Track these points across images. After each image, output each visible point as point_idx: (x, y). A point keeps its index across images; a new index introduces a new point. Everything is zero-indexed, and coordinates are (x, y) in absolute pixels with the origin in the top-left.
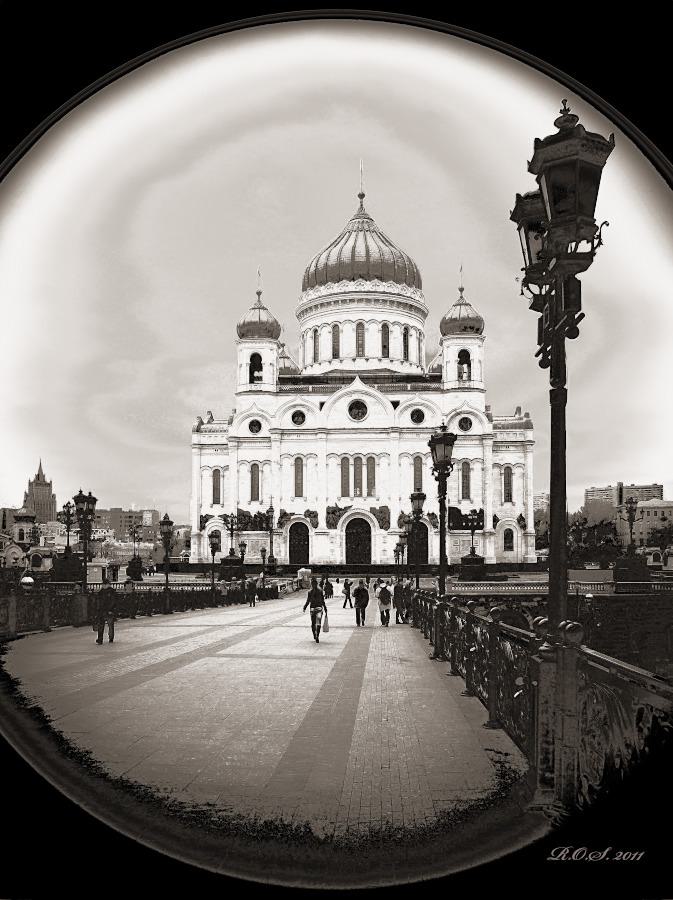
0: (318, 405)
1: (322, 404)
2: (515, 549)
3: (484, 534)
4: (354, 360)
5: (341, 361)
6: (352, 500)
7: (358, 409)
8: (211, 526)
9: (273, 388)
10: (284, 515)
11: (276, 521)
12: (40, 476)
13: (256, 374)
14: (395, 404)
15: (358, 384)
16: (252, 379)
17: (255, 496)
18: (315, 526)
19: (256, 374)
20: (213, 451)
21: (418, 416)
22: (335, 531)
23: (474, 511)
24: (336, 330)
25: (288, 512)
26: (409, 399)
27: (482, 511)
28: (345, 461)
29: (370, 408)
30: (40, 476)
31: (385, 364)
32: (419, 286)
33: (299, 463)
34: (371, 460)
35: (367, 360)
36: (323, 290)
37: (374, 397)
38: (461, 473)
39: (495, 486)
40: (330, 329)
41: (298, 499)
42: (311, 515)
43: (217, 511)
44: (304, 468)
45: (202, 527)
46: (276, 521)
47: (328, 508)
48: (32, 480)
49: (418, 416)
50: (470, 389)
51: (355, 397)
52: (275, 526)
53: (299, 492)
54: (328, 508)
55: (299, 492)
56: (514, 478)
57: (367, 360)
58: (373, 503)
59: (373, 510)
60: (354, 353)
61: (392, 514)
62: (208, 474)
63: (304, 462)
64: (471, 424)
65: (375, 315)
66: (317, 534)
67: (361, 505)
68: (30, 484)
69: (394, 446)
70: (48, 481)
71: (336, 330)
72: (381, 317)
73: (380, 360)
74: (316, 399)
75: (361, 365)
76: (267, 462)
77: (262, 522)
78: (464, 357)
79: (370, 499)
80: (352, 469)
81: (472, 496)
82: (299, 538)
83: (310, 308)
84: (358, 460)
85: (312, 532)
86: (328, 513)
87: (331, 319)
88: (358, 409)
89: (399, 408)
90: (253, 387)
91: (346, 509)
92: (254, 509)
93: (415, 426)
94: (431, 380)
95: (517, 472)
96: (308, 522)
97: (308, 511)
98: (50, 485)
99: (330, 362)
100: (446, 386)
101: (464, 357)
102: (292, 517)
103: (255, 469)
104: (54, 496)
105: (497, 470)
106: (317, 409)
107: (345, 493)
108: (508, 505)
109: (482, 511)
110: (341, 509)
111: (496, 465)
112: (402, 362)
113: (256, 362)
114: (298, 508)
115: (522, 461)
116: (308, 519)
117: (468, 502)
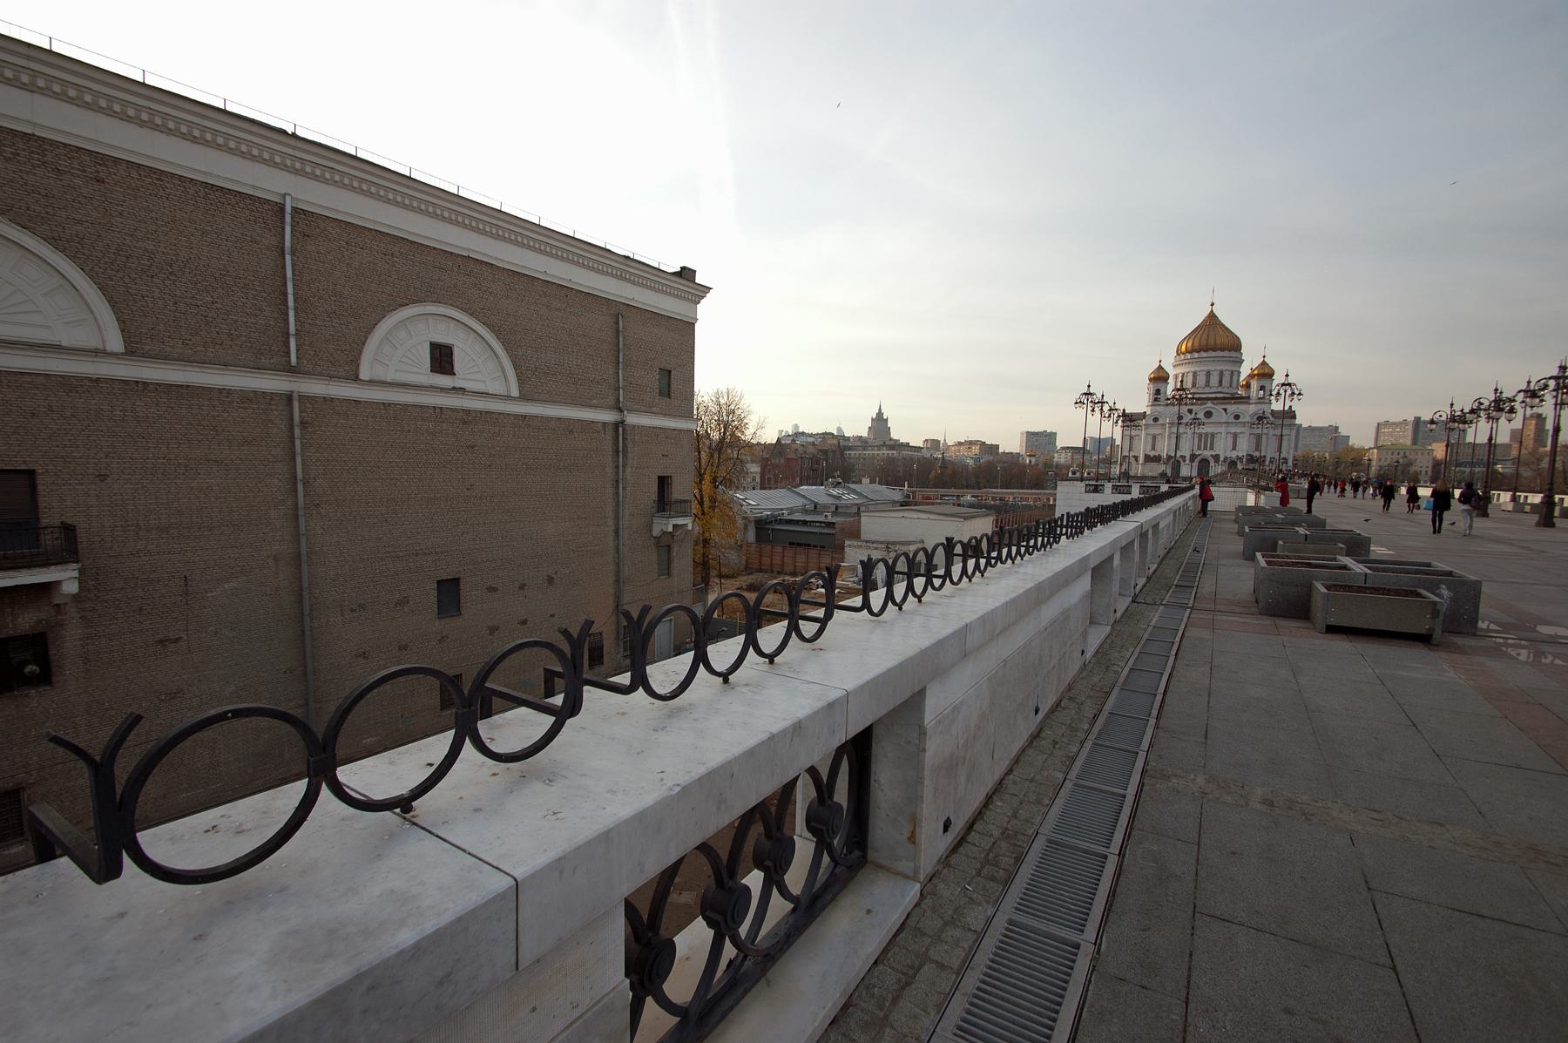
7: (1208, 414)
12: (880, 414)
14: (1225, 410)
15: (1209, 404)
17: (1153, 449)
21: (1237, 417)
26: (1232, 408)
29: (1214, 414)
30: (880, 414)
31: (1220, 389)
34: (1213, 435)
39: (1274, 443)
40: (1191, 374)
42: (1183, 457)
48: (874, 417)
49: (1237, 417)
51: (1207, 410)
59: (1212, 456)
65: (1215, 368)
67: (1207, 453)
68: (873, 419)
69: (1223, 429)
70: (885, 417)
72: (1219, 368)
75: (1207, 390)
76: (1158, 435)
77: (1157, 459)
82: (1176, 466)
85: (1182, 463)
88: (1208, 414)
90: (1156, 403)
91: (1199, 455)
92: (1152, 454)
94: (1245, 400)
103: (1154, 437)
105: (1274, 437)
106: (1188, 414)
107: (1199, 449)
111: (1274, 435)
113: (1158, 392)
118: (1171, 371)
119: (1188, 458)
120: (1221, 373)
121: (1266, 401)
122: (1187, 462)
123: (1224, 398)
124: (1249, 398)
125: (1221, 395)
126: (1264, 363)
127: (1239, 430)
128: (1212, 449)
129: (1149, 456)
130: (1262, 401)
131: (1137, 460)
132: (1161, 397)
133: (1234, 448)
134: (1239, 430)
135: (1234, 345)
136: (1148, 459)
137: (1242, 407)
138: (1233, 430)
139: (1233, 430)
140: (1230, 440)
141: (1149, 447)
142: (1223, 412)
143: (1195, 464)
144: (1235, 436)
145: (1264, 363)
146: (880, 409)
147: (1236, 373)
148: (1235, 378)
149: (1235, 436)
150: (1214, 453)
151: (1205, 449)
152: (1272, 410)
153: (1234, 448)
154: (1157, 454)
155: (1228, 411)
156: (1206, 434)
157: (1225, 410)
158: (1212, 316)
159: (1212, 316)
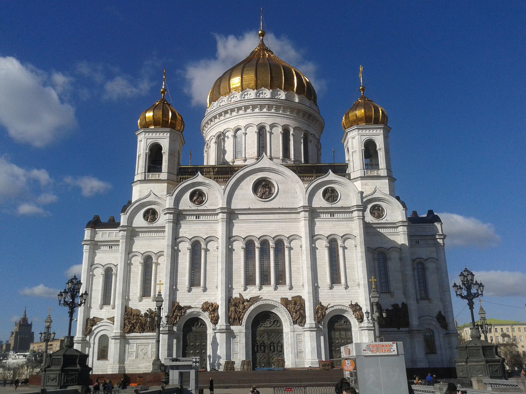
2: (439, 352)
3: (410, 332)
5: (245, 160)
6: (260, 288)
11: (164, 314)
12: (25, 320)
18: (215, 321)
20: (107, 248)
22: (239, 327)
23: (395, 306)
25: (182, 304)
27: (404, 305)
28: (249, 246)
30: (25, 320)
34: (279, 244)
38: (376, 263)
41: (194, 289)
46: (164, 314)
48: (18, 322)
50: (379, 177)
52: (164, 320)
56: (428, 273)
57: (271, 159)
58: (284, 292)
59: (285, 302)
60: (256, 155)
62: (99, 273)
64: (383, 210)
70: (30, 323)
79: (280, 288)
81: (392, 290)
84: (264, 243)
93: (329, 206)
95: (430, 265)
96: (205, 317)
97: (206, 303)
98: (30, 326)
102: (188, 311)
104: (33, 333)
107: (249, 281)
108: (425, 303)
109: (404, 305)
110: (244, 301)
115: (434, 255)
116: (206, 314)
117: (388, 295)
119: (221, 312)
122: (222, 322)
128: (280, 279)
129: (137, 314)
130: (375, 173)
143: (239, 330)
146: (25, 315)
147: (310, 138)
150: (289, 295)
151: (265, 280)
154: (153, 306)
156: (264, 243)
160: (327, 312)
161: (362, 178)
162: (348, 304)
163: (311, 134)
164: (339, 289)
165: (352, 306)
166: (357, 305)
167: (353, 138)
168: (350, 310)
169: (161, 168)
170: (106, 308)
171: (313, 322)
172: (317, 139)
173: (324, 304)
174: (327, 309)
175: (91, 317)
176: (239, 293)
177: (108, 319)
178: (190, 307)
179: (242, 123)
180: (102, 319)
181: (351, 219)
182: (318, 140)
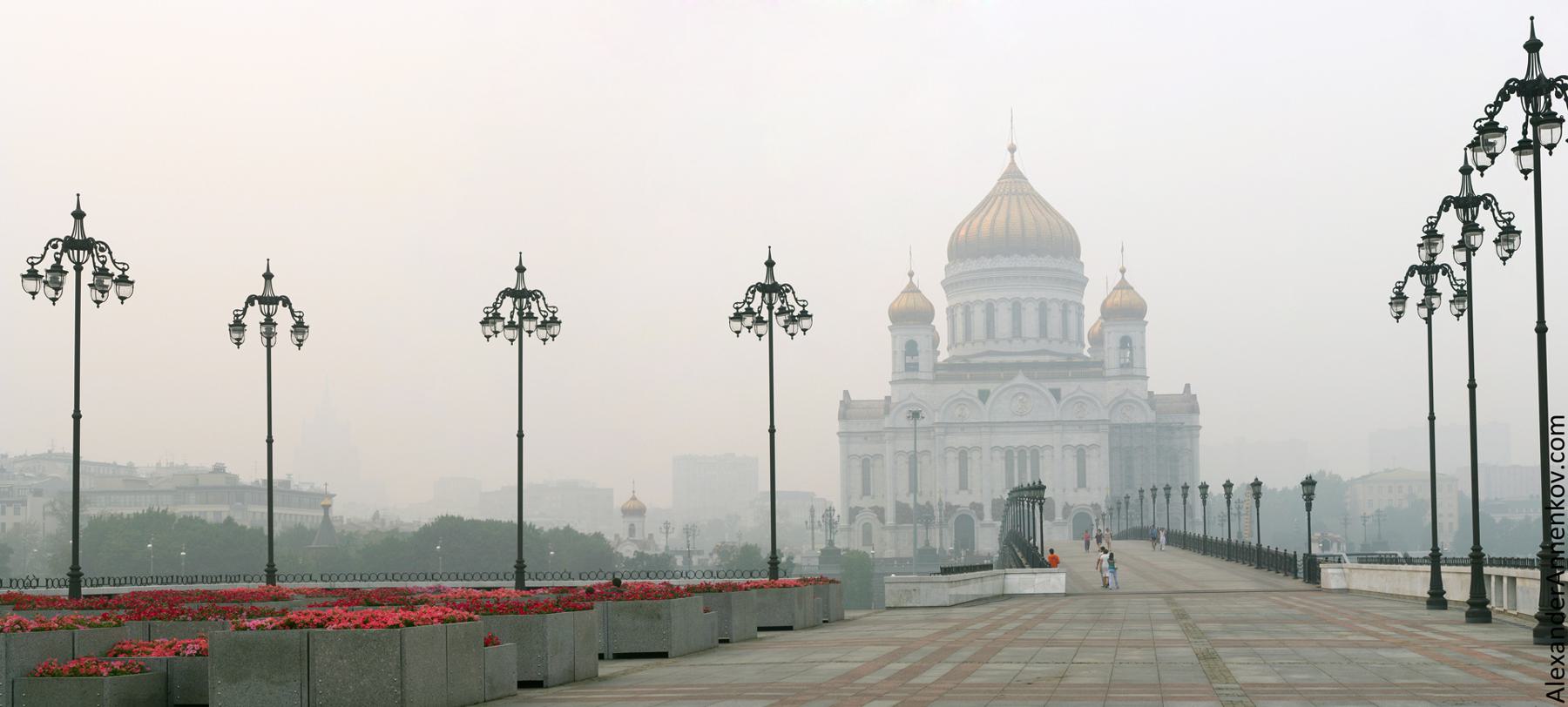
0: (976, 394)
1: (984, 395)
4: (1010, 341)
5: (997, 342)
8: (861, 519)
9: (930, 376)
10: (950, 509)
13: (909, 360)
14: (1056, 393)
16: (912, 367)
18: (981, 517)
19: (909, 360)
24: (990, 309)
31: (1043, 344)
32: (1078, 255)
33: (963, 455)
35: (1024, 341)
36: (973, 265)
37: (1038, 390)
42: (977, 507)
43: (867, 503)
44: (969, 461)
45: (851, 520)
47: (994, 500)
50: (1133, 377)
53: (963, 485)
54: (994, 500)
55: (963, 485)
57: (1024, 341)
61: (1056, 503)
63: (969, 456)
66: (983, 526)
71: (990, 309)
73: (1038, 341)
74: (973, 389)
75: (1017, 346)
78: (1126, 343)
80: (1016, 462)
83: (962, 282)
85: (977, 523)
86: (993, 505)
87: (984, 296)
89: (1063, 402)
90: (910, 375)
94: (1091, 369)
96: (973, 514)
97: (973, 503)
99: (984, 343)
100: (1108, 373)
101: (1126, 343)
102: (959, 509)
106: (979, 403)
112: (1061, 342)
113: (911, 348)
114: (962, 500)
116: (974, 512)
118: (940, 303)
120: (1043, 309)
121: (1138, 372)
123: (1052, 365)
124: (1101, 364)
125: (1047, 358)
126: (1123, 286)
127: (1087, 439)
131: (882, 520)
132: (924, 361)
133: (1082, 483)
134: (1087, 439)
135: (1063, 244)
136: (903, 513)
137: (1090, 386)
138: (1077, 439)
139: (1077, 439)
140: (1071, 464)
141: (904, 485)
142: (1053, 400)
144: (1081, 453)
145: (1123, 286)
147: (1072, 308)
148: (1072, 318)
149: (1081, 453)
152: (1151, 393)
153: (1082, 483)
155: (1063, 394)
156: (1022, 450)
157: (1056, 393)
158: (1013, 175)
159: (1013, 175)
160: (1073, 510)
161: (1114, 378)
162: (1090, 504)
163: (1071, 302)
164: (1082, 492)
165: (1092, 505)
166: (1097, 504)
167: (1109, 333)
168: (1091, 509)
169: (917, 364)
170: (866, 498)
171: (1061, 518)
172: (1077, 304)
173: (1070, 504)
174: (1072, 507)
175: (853, 507)
176: (1001, 496)
177: (870, 508)
178: (959, 506)
179: (995, 296)
180: (862, 509)
181: (1097, 431)
182: (1081, 307)
